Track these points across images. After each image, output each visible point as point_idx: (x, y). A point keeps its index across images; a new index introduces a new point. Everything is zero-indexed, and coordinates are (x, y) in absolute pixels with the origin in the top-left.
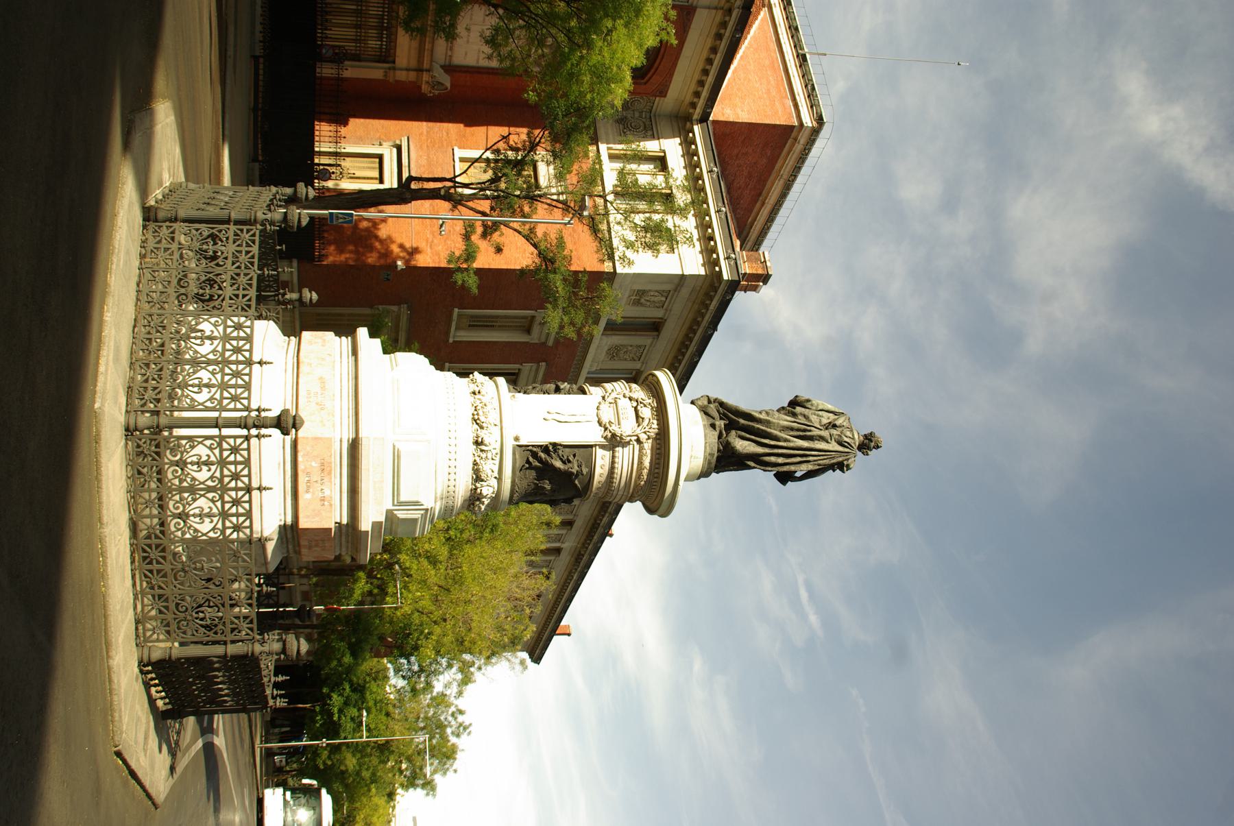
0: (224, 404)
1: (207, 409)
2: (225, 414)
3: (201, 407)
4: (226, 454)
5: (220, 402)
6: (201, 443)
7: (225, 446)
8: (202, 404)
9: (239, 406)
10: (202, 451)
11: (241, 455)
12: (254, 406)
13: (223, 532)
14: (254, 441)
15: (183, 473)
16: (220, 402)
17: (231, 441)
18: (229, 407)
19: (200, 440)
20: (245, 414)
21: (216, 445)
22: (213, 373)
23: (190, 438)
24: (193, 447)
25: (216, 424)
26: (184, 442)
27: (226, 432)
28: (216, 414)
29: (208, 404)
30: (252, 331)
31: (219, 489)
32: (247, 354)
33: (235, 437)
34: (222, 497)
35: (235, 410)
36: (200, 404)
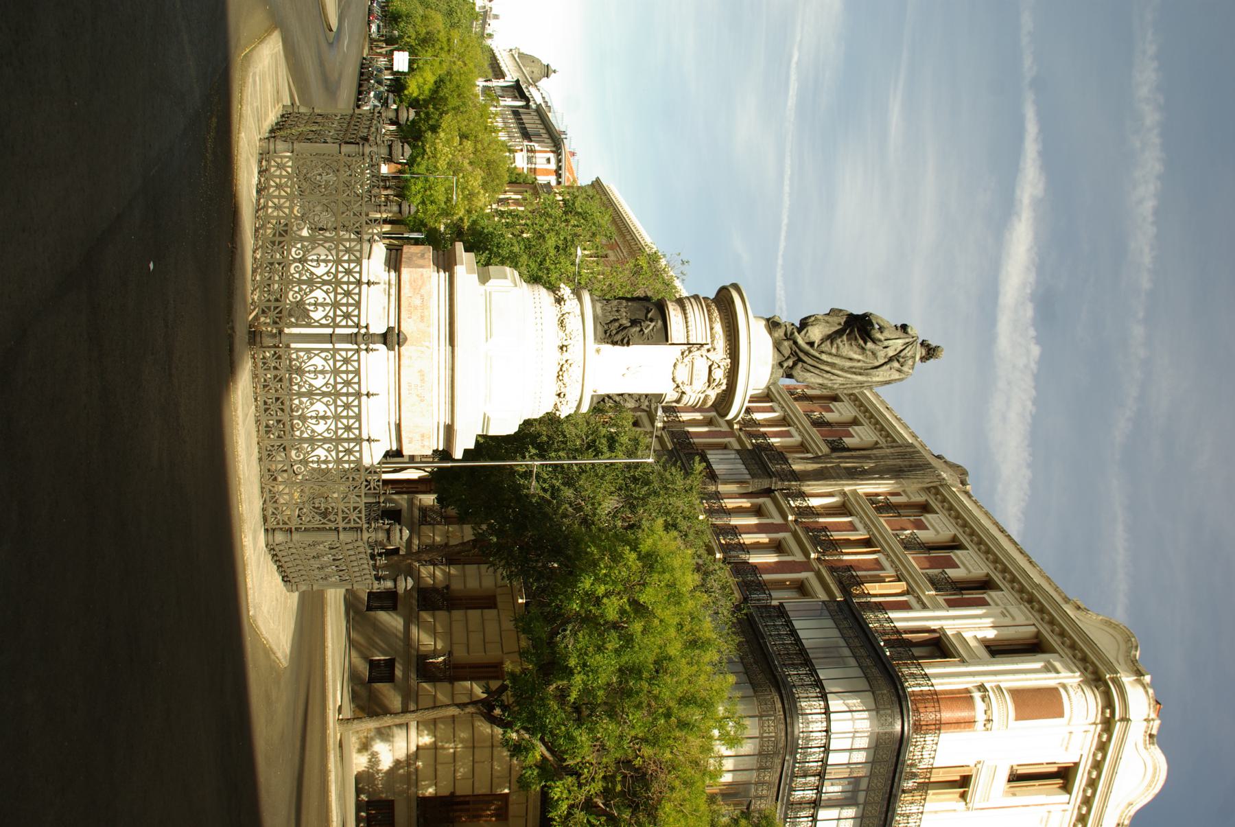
1: (322, 326)
2: (338, 331)
3: (316, 324)
4: (338, 364)
5: (334, 320)
6: (317, 355)
7: (338, 357)
8: (318, 322)
9: (350, 323)
10: (318, 362)
13: (336, 432)
14: (363, 353)
15: (302, 380)
16: (334, 320)
17: (343, 353)
18: (341, 324)
19: (316, 352)
20: (355, 330)
21: (330, 356)
23: (308, 351)
24: (310, 358)
25: (330, 338)
26: (302, 354)
28: (329, 331)
29: (323, 321)
31: (333, 394)
33: (347, 350)
34: (335, 401)
35: (347, 326)
36: (316, 321)
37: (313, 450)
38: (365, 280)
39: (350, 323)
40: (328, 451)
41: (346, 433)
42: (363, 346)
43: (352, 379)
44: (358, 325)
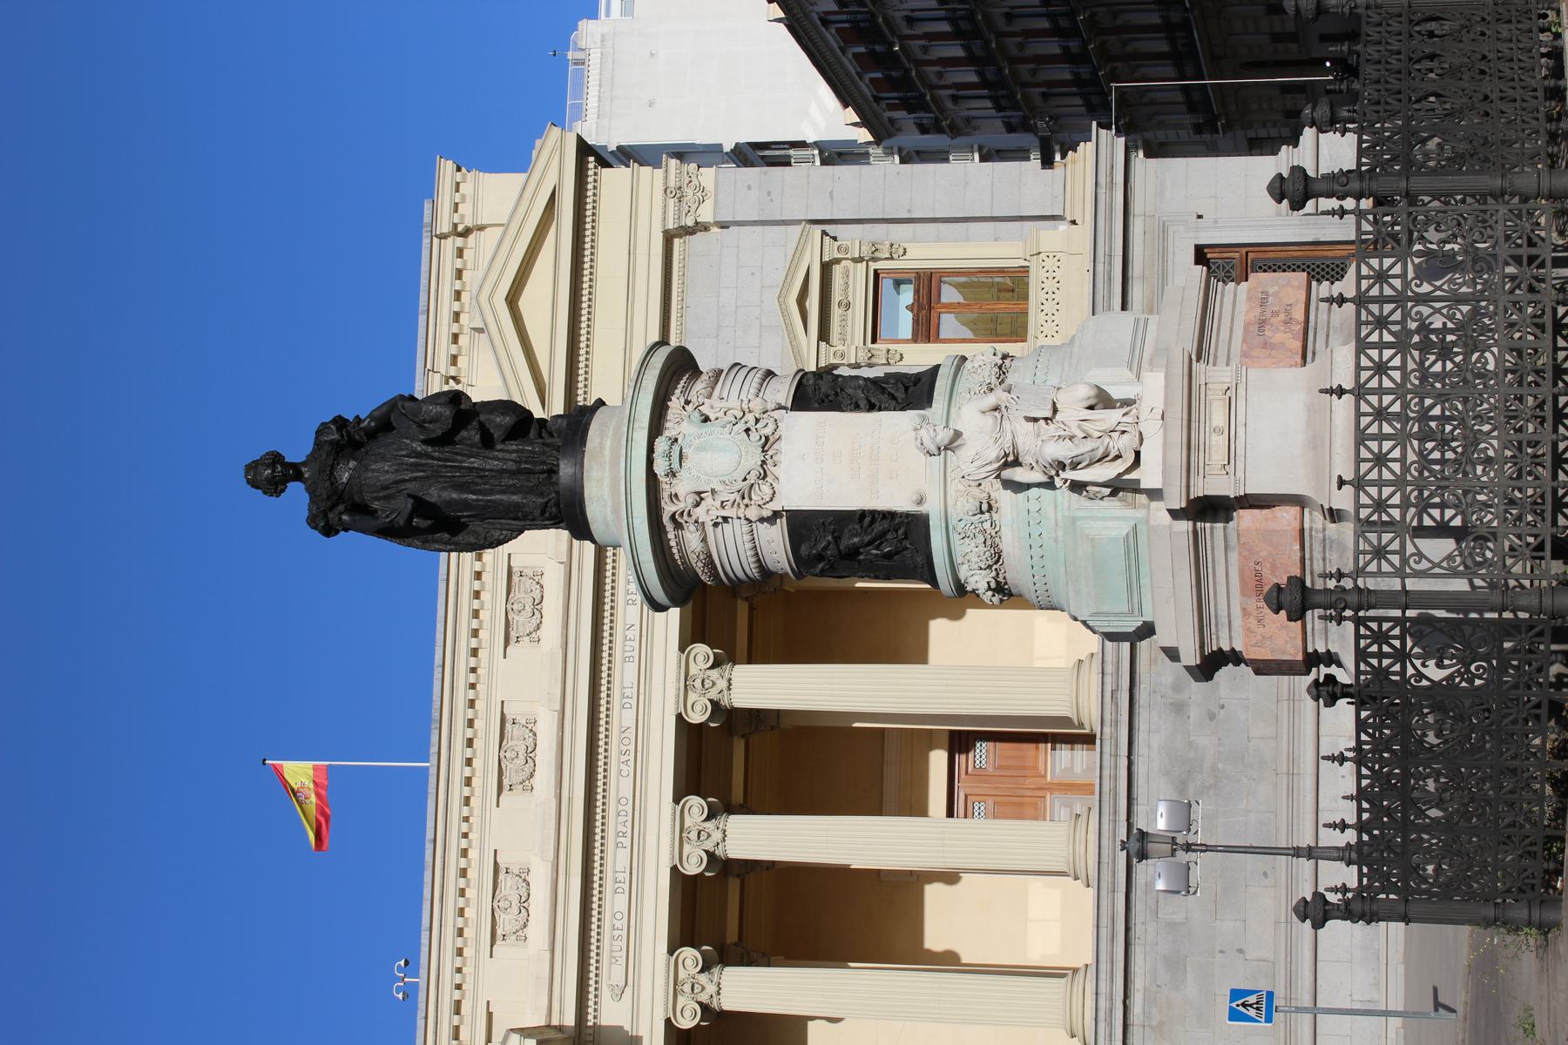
0: (1399, 664)
2: (1397, 613)
9: (1374, 626)
11: (1371, 359)
12: (1349, 626)
22: (1420, 676)
27: (1396, 584)
30: (1357, 543)
32: (1362, 631)
33: (1379, 573)
35: (1380, 620)
37: (1450, 678)
38: (1349, 308)
39: (1374, 626)
40: (1420, 555)
41: (1384, 542)
42: (1348, 583)
43: (1370, 470)
44: (1358, 622)
